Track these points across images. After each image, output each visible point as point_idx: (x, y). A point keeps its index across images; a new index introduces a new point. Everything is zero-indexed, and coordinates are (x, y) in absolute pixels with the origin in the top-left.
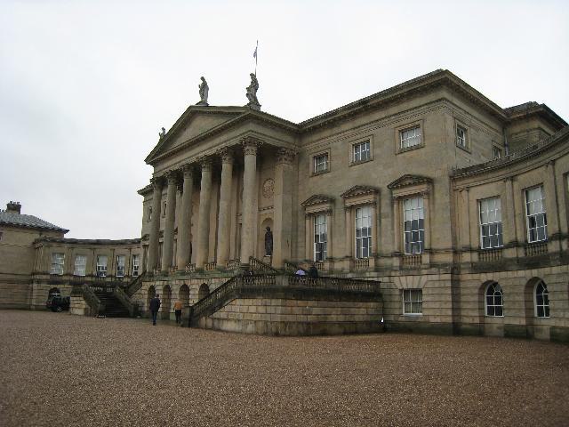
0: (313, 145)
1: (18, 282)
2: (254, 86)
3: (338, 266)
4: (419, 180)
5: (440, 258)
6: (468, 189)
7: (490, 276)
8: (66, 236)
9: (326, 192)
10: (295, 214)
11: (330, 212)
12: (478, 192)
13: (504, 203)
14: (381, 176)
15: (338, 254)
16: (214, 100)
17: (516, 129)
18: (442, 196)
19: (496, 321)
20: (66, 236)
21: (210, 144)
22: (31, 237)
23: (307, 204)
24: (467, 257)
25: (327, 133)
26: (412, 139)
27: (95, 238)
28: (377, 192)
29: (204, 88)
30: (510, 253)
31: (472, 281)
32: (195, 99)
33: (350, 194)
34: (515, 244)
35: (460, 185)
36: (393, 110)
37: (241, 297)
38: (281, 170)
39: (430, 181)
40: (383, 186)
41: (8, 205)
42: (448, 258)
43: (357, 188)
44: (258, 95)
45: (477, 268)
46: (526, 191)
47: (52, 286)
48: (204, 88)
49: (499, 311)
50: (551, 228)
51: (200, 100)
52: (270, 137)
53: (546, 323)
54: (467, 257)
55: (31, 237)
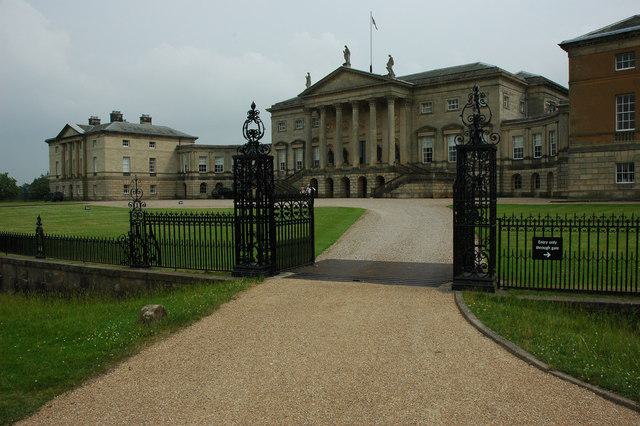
0: (421, 96)
1: (170, 179)
2: (391, 62)
3: (438, 165)
6: (508, 131)
7: (517, 172)
8: (197, 142)
10: (411, 137)
11: (433, 137)
12: (513, 132)
13: (525, 139)
15: (438, 159)
16: (355, 65)
17: (531, 91)
19: (519, 191)
20: (197, 142)
21: (358, 93)
22: (173, 145)
23: (422, 129)
24: (507, 163)
25: (430, 91)
27: (227, 144)
29: (347, 53)
30: (526, 162)
32: (340, 62)
33: (446, 128)
34: (528, 158)
35: (505, 128)
37: (409, 183)
38: (405, 110)
41: (142, 118)
43: (451, 125)
44: (394, 68)
45: (511, 168)
46: (535, 135)
47: (202, 181)
48: (347, 53)
49: (520, 187)
50: (543, 153)
51: (344, 61)
52: (400, 93)
53: (538, 191)
54: (507, 163)
55: (173, 145)
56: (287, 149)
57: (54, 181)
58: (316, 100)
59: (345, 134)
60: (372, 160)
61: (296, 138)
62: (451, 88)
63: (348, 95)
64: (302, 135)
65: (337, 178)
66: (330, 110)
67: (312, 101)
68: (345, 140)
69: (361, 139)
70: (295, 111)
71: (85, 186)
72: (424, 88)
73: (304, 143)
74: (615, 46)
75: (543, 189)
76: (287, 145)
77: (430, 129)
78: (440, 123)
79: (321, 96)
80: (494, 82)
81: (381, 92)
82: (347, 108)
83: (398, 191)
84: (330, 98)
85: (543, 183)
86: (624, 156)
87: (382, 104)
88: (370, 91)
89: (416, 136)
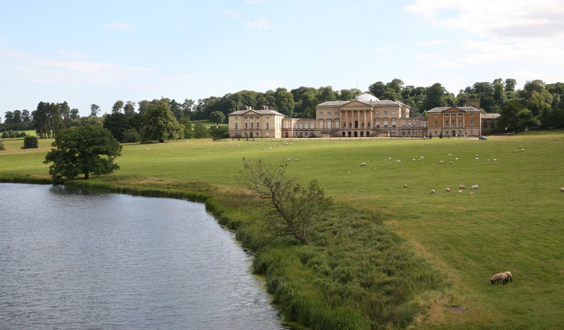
4: (396, 119)
5: (398, 129)
9: (379, 117)
14: (389, 117)
18: (398, 121)
21: (360, 108)
26: (394, 113)
28: (389, 119)
30: (406, 129)
31: (401, 131)
36: (392, 108)
39: (397, 119)
40: (390, 119)
42: (399, 129)
45: (402, 130)
54: (401, 129)
56: (324, 121)
57: (234, 131)
58: (345, 108)
59: (350, 118)
60: (366, 126)
61: (328, 118)
62: (385, 108)
63: (356, 108)
64: (336, 117)
65: (353, 132)
66: (349, 112)
67: (341, 108)
68: (350, 120)
69: (356, 120)
70: (327, 109)
71: (262, 132)
72: (377, 107)
73: (332, 120)
74: (434, 113)
75: (415, 135)
76: (324, 120)
77: (379, 119)
78: (382, 117)
79: (347, 107)
80: (397, 108)
81: (368, 109)
82: (355, 112)
83: (378, 135)
84: (349, 108)
85: (415, 133)
86: (436, 130)
87: (368, 111)
88: (365, 108)
89: (374, 120)
